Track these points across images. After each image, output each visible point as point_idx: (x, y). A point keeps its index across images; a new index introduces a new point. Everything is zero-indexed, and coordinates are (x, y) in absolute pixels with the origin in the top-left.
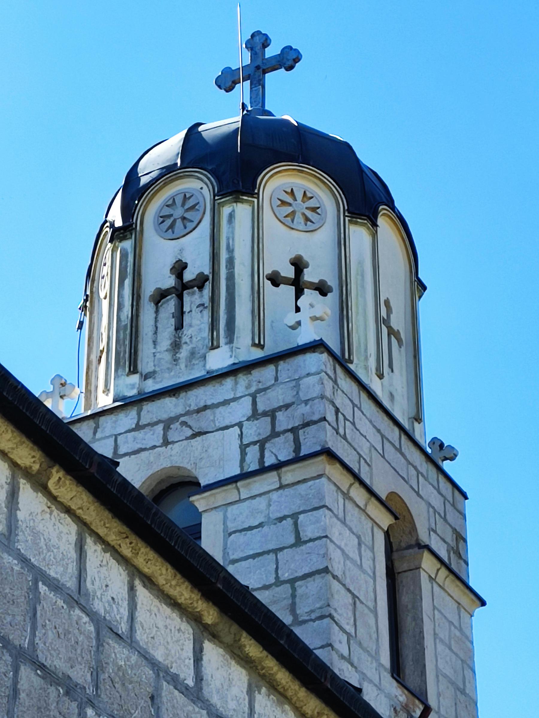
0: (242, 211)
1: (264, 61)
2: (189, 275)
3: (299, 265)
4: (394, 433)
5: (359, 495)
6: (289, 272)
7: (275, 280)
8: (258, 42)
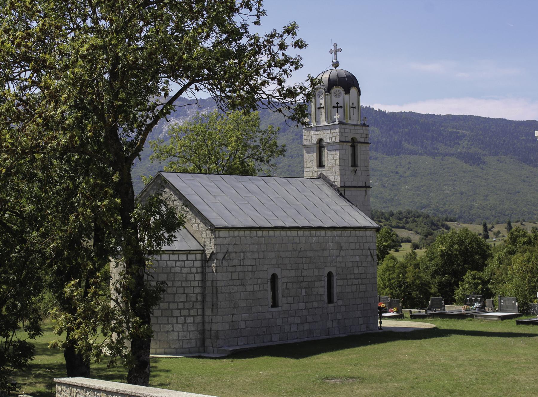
0: (329, 96)
1: (336, 51)
2: (322, 106)
3: (337, 103)
4: (353, 127)
5: (345, 144)
6: (336, 105)
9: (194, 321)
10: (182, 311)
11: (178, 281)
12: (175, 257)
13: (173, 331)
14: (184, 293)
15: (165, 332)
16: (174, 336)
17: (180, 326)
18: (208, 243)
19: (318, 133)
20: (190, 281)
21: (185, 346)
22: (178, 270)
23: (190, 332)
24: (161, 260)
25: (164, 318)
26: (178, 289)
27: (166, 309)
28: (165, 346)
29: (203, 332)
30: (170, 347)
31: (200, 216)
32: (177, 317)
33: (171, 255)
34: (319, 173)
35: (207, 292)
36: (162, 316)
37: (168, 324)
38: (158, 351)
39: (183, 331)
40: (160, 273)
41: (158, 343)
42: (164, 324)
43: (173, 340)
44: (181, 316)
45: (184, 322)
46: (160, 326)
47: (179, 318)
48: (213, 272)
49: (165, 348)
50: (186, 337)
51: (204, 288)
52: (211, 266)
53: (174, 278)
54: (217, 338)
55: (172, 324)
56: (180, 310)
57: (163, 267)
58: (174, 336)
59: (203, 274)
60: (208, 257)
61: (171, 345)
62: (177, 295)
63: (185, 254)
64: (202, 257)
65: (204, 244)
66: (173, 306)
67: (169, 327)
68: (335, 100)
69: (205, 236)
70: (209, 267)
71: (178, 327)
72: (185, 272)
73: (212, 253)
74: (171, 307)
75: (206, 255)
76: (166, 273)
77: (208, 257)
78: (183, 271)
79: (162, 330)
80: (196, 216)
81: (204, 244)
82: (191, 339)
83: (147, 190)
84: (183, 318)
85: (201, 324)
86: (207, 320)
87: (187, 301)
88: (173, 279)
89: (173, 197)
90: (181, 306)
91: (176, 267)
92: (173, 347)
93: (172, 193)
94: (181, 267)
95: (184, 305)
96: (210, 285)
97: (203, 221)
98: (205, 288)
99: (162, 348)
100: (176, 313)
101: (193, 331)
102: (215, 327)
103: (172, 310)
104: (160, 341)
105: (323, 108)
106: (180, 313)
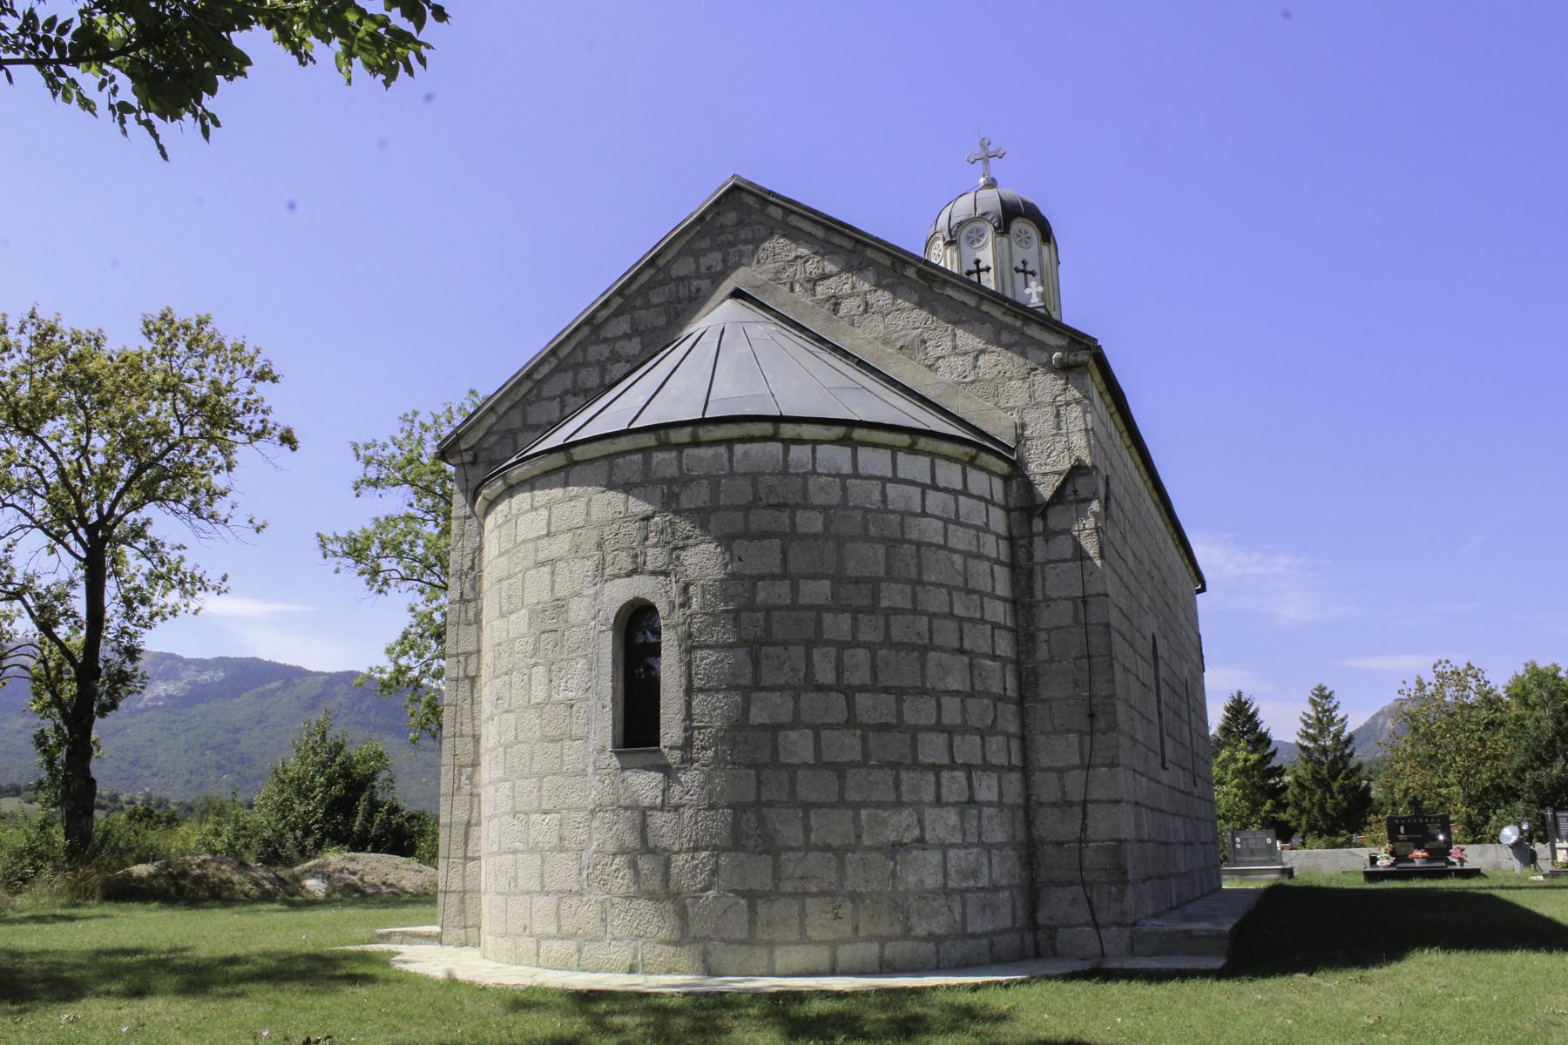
0: (1005, 240)
7: (1017, 270)
8: (985, 144)
9: (1001, 795)
10: (957, 739)
11: (940, 585)
12: (914, 467)
13: (921, 840)
14: (961, 651)
15: (878, 849)
16: (923, 871)
17: (952, 816)
18: (1039, 424)
20: (982, 594)
21: (977, 925)
22: (931, 530)
23: (988, 847)
24: (856, 475)
25: (877, 775)
26: (937, 624)
27: (885, 727)
28: (884, 929)
29: (1030, 851)
30: (907, 933)
31: (986, 318)
32: (937, 769)
33: (901, 456)
35: (1042, 652)
36: (864, 763)
37: (899, 804)
38: (846, 954)
39: (965, 846)
40: (852, 538)
41: (847, 908)
42: (880, 805)
43: (923, 894)
44: (953, 766)
45: (965, 798)
46: (856, 819)
47: (945, 775)
48: (1080, 555)
49: (883, 940)
50: (975, 874)
51: (1024, 637)
52: (1068, 531)
53: (919, 566)
54: (1118, 873)
55: (916, 805)
56: (950, 731)
57: (866, 511)
58: (923, 871)
59: (1021, 570)
60: (1046, 490)
61: (914, 920)
62: (932, 655)
63: (956, 460)
64: (1006, 493)
65: (1019, 438)
66: (918, 711)
67: (899, 825)
68: (1020, 253)
69: (1021, 399)
70: (1048, 535)
71: (942, 824)
72: (960, 547)
73: (1078, 469)
74: (910, 718)
75: (1029, 487)
76: (882, 539)
77: (1046, 490)
78: (954, 542)
79: (866, 841)
80: (956, 323)
81: (1019, 438)
82: (996, 889)
83: (661, 262)
84: (960, 775)
85: (1020, 814)
86: (1048, 789)
87: (972, 694)
88: (914, 576)
89: (810, 267)
90: (952, 711)
91: (924, 514)
92: (921, 930)
93: (803, 251)
94: (946, 521)
95: (964, 711)
96: (1067, 620)
97: (1006, 337)
98: (1031, 638)
99: (870, 939)
100: (933, 748)
101: (999, 846)
102: (1102, 825)
103: (915, 730)
104: (855, 897)
105: (988, 269)
106: (951, 747)
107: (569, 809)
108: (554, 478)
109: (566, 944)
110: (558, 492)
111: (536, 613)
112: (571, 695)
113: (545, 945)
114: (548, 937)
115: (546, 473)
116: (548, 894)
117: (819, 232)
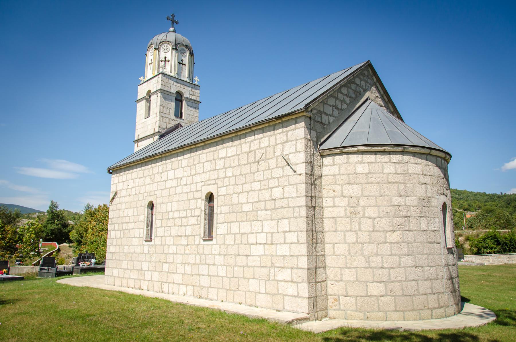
19: (179, 85)
34: (177, 123)
107: (438, 266)
108: (423, 156)
109: (441, 309)
110: (424, 161)
111: (421, 199)
112: (435, 229)
113: (434, 311)
114: (436, 308)
115: (420, 153)
116: (434, 294)
117: (382, 92)
